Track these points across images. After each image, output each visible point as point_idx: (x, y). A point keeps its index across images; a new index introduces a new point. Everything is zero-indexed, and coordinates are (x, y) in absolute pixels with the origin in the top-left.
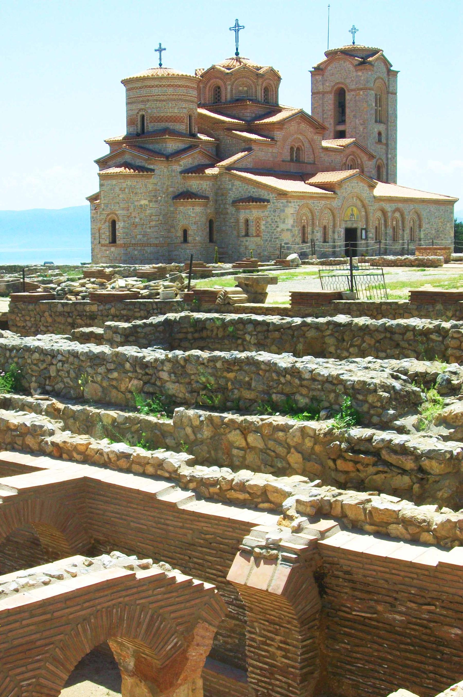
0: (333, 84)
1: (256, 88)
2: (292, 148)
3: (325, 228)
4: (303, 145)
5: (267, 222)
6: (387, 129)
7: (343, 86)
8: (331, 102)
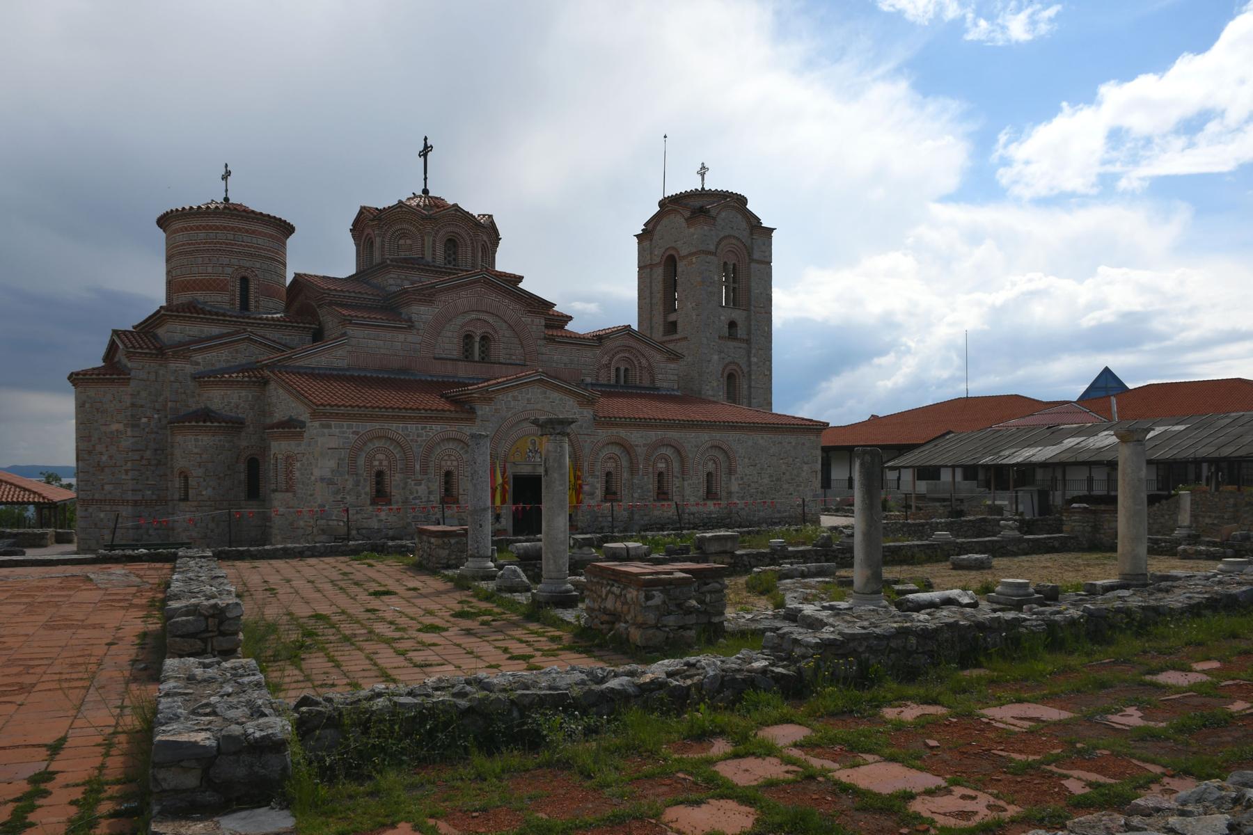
0: (663, 250)
1: (423, 240)
2: (468, 337)
3: (448, 474)
4: (496, 332)
5: (302, 465)
7: (673, 252)
8: (660, 278)
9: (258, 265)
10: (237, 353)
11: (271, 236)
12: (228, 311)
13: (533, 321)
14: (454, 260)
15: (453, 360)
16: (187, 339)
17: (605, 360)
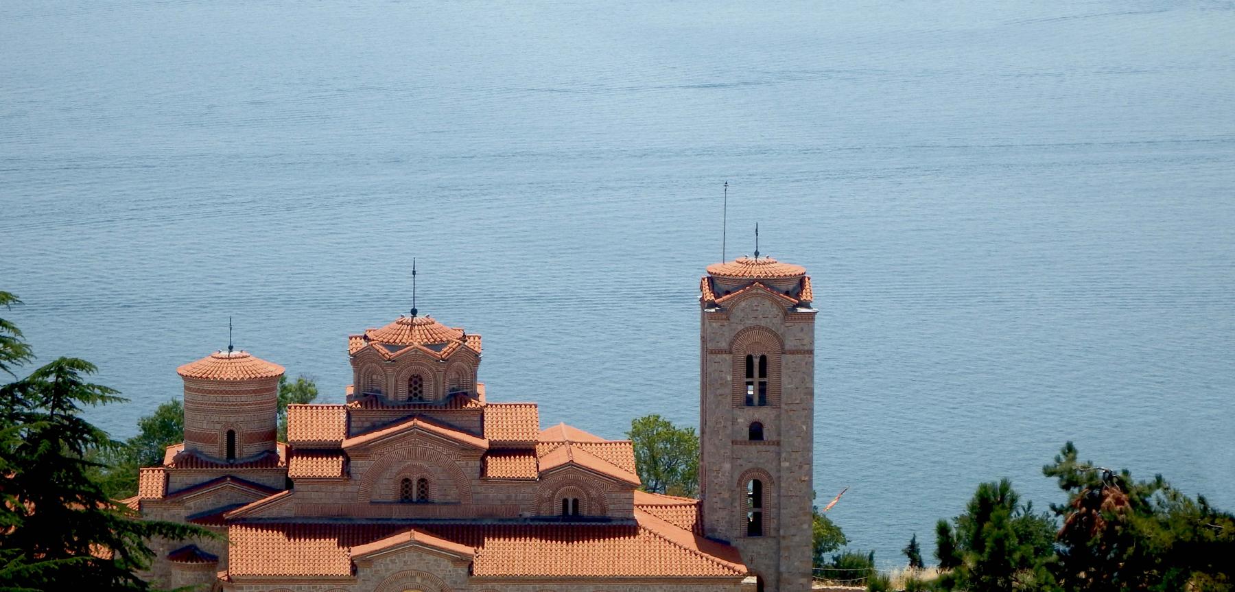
1: (387, 381)
2: (406, 482)
6: (778, 417)
9: (242, 419)
10: (220, 496)
11: (254, 392)
12: (218, 459)
13: (467, 464)
14: (421, 392)
15: (391, 503)
16: (185, 487)
17: (548, 493)
